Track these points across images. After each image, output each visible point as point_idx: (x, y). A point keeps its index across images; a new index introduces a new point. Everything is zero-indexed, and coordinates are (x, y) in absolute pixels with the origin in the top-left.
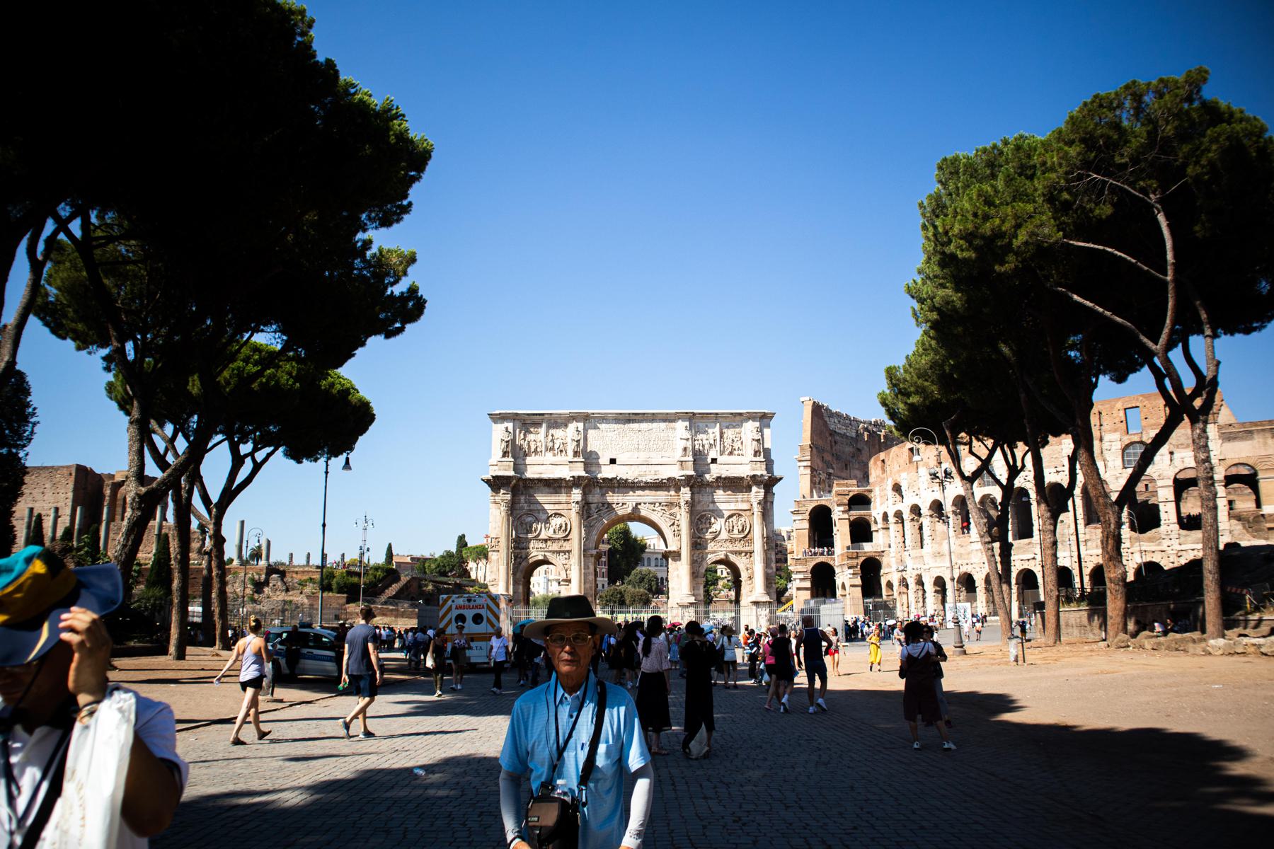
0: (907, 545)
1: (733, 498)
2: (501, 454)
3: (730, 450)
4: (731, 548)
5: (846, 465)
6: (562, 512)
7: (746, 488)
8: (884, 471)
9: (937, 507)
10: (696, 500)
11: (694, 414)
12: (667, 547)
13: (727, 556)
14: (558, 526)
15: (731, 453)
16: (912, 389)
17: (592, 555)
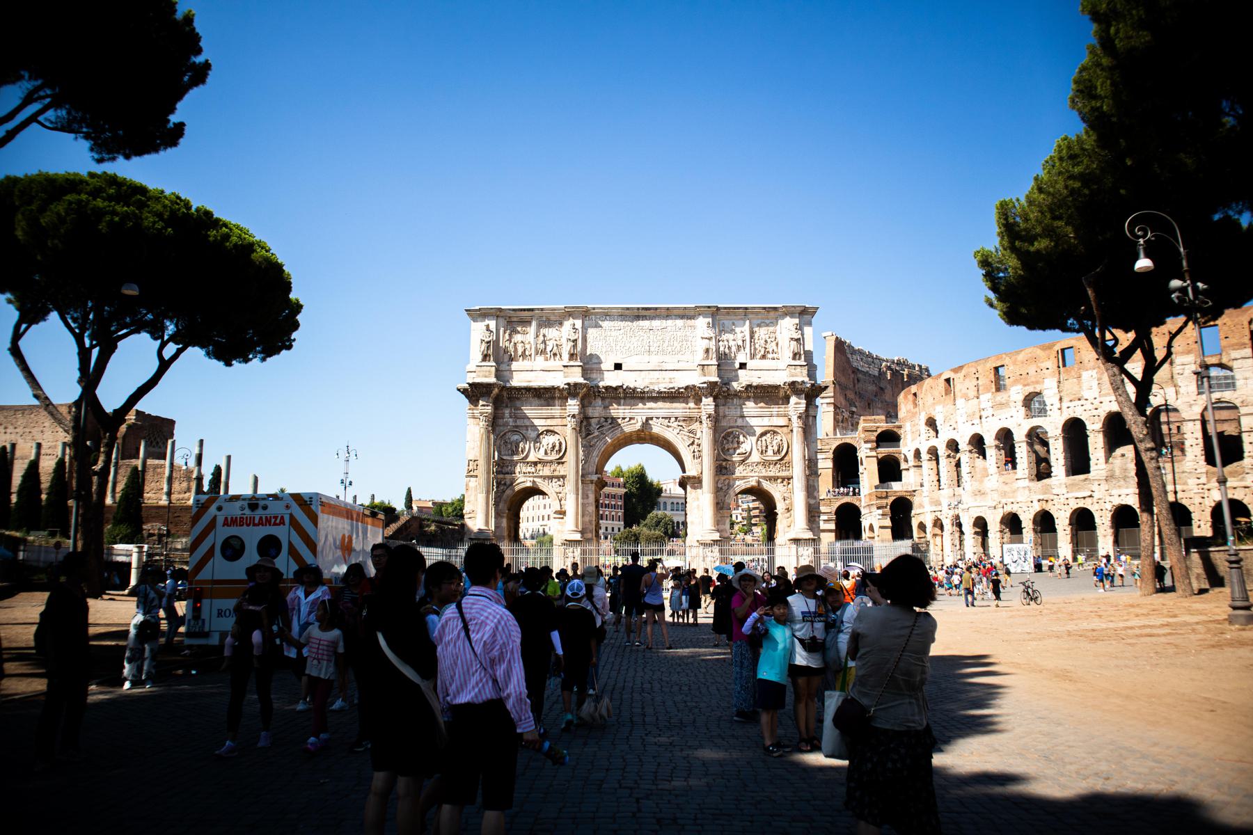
0: (942, 483)
1: (766, 411)
2: (480, 357)
3: (762, 353)
4: (764, 474)
5: (869, 404)
6: (556, 429)
7: (782, 399)
8: (915, 405)
9: (978, 443)
10: (721, 414)
11: (718, 309)
12: (684, 471)
13: (759, 482)
14: (550, 446)
15: (764, 357)
16: (1039, 230)
17: (592, 482)
